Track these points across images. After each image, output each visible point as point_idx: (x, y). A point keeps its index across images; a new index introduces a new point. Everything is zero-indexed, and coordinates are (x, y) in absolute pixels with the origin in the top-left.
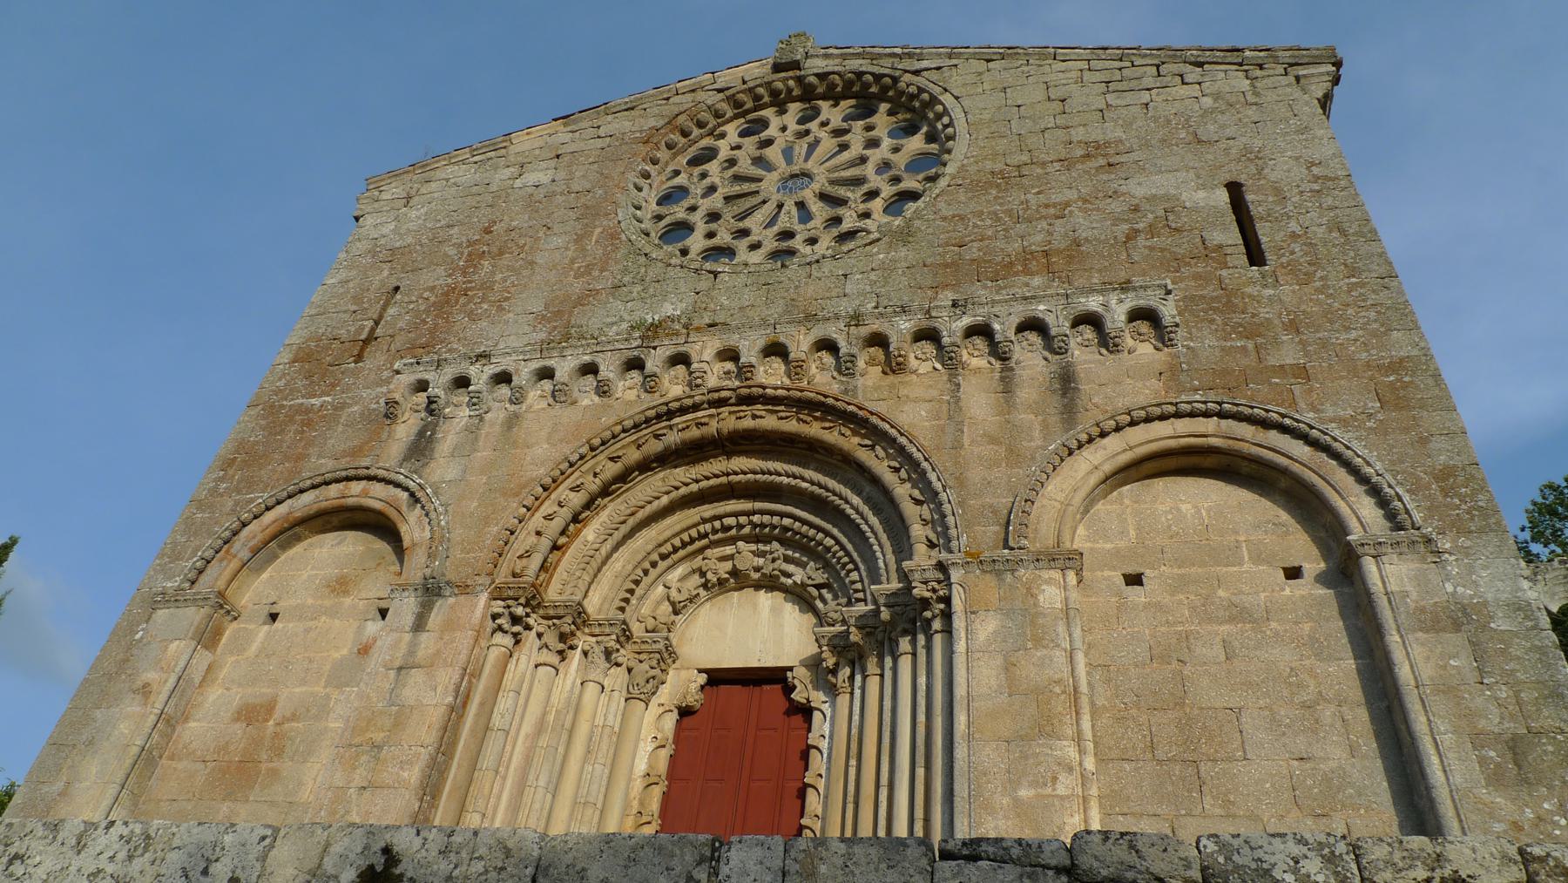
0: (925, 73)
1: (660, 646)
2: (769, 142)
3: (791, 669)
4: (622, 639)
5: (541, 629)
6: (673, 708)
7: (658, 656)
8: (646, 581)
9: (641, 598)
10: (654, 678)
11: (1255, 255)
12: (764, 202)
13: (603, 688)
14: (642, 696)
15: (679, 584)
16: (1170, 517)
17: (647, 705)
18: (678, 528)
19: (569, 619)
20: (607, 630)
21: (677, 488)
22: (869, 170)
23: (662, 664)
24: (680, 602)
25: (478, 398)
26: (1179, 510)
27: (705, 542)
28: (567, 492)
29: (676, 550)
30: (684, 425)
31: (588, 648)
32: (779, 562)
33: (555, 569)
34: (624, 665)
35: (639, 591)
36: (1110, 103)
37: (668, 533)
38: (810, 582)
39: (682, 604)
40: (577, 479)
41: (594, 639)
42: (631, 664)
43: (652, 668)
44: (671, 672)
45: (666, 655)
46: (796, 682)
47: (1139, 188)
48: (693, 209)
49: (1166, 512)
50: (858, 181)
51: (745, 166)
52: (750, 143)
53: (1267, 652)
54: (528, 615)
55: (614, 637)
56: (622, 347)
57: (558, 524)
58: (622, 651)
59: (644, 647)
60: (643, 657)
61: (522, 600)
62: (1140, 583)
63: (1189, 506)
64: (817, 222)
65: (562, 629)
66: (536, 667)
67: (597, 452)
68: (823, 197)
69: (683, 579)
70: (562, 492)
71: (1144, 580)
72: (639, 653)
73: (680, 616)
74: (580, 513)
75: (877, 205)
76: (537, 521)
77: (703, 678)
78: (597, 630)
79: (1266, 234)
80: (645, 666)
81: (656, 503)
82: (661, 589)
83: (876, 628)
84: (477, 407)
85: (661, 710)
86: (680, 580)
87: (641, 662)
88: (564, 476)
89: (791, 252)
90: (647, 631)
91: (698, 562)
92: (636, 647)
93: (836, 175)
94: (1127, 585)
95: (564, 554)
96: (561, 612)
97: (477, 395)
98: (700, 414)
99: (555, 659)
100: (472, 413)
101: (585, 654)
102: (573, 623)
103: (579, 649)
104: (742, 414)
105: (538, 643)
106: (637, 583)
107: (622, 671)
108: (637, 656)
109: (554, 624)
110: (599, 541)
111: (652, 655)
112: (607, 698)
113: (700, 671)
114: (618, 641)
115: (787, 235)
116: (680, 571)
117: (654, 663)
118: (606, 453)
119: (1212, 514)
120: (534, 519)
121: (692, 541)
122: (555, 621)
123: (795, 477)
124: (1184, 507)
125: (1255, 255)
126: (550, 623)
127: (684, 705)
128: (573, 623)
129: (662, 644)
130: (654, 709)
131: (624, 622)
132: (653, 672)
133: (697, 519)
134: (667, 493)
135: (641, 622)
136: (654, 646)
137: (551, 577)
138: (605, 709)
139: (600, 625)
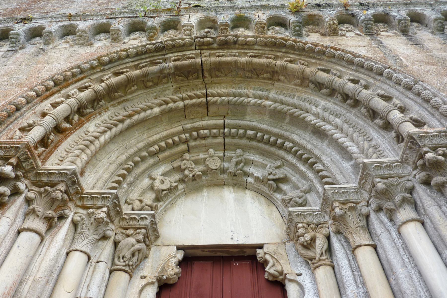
1: (147, 222)
3: (261, 247)
4: (112, 213)
5: (31, 195)
6: (155, 280)
7: (143, 231)
8: (138, 171)
9: (131, 184)
10: (139, 250)
13: (89, 258)
14: (127, 269)
15: (162, 177)
17: (131, 277)
18: (165, 133)
19: (62, 187)
20: (99, 203)
21: (167, 103)
23: (147, 240)
24: (163, 190)
25: (16, 38)
27: (183, 147)
28: (76, 90)
29: (161, 150)
30: (176, 58)
31: (79, 219)
32: (242, 164)
33: (56, 147)
34: (112, 239)
35: (130, 179)
37: (157, 137)
38: (271, 177)
39: (165, 192)
40: (86, 82)
41: (84, 212)
42: (119, 237)
43: (138, 242)
44: (153, 249)
45: (150, 232)
46: (268, 257)
54: (17, 178)
55: (105, 209)
56: (130, 16)
57: (62, 109)
58: (111, 226)
59: (131, 223)
60: (130, 232)
61: (13, 160)
65: (53, 195)
66: (19, 232)
67: (106, 67)
70: (72, 90)
72: (126, 229)
73: (161, 203)
74: (85, 107)
76: (46, 105)
77: (180, 255)
78: (89, 203)
80: (132, 240)
81: (149, 112)
83: (357, 203)
84: (15, 45)
85: (144, 282)
86: (163, 175)
87: (128, 236)
88: (75, 79)
90: (133, 210)
91: (176, 164)
92: (124, 224)
95: (66, 137)
96: (54, 179)
97: (15, 36)
98: (188, 53)
99: (41, 226)
100: (10, 49)
101: (75, 224)
102: (66, 192)
103: (70, 219)
105: (25, 206)
106: (129, 170)
107: (108, 246)
108: (124, 231)
109: (46, 191)
110: (99, 130)
111: (139, 231)
112: (92, 269)
113: (179, 248)
114: (108, 215)
116: (163, 169)
117: (141, 237)
118: (112, 70)
120: (43, 104)
121: (175, 144)
122: (47, 188)
123: (260, 98)
126: (42, 189)
127: (165, 277)
128: (66, 192)
129: (149, 221)
130: (138, 283)
131: (116, 197)
132: (138, 246)
133: (180, 128)
134: (160, 105)
135: (129, 204)
136: (141, 223)
137: (51, 153)
138: (88, 279)
139: (93, 198)
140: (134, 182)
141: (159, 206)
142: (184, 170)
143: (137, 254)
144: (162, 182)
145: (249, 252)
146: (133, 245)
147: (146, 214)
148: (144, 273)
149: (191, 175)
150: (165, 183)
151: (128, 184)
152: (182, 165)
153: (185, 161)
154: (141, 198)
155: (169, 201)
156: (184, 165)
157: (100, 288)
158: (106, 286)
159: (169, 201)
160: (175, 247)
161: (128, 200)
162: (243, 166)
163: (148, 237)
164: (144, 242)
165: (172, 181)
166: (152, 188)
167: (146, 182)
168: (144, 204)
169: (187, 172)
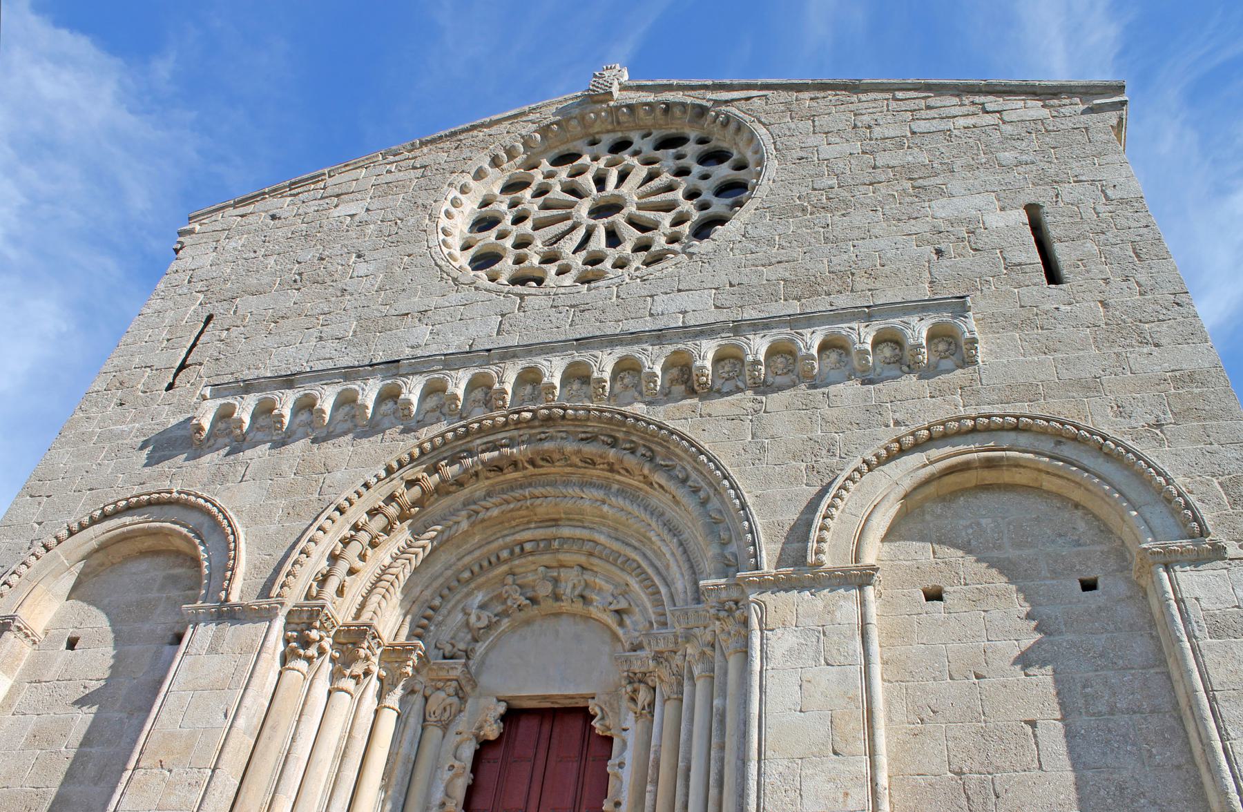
0: (735, 103)
2: (580, 172)
9: (439, 624)
11: (1053, 276)
12: (573, 228)
16: (970, 531)
22: (679, 194)
23: (460, 692)
24: (480, 629)
26: (978, 524)
36: (915, 130)
39: (482, 631)
42: (428, 692)
43: (449, 695)
47: (941, 209)
48: (501, 236)
49: (966, 527)
50: (668, 207)
51: (557, 193)
52: (563, 172)
53: (1062, 664)
62: (940, 598)
63: (990, 520)
64: (626, 248)
68: (632, 222)
69: (483, 607)
71: (944, 595)
73: (480, 644)
75: (686, 229)
77: (502, 708)
79: (1061, 252)
80: (442, 695)
82: (460, 616)
89: (600, 276)
90: (445, 657)
93: (643, 200)
94: (927, 600)
104: (543, 436)
111: (449, 683)
115: (595, 260)
117: (451, 691)
119: (1011, 527)
124: (984, 521)
125: (1053, 276)
132: (449, 700)
135: (439, 649)
138: (400, 735)
140: (443, 621)
141: (476, 648)
142: (506, 599)
143: (448, 708)
144: (479, 618)
145: (581, 704)
146: (444, 700)
147: (455, 664)
148: (460, 729)
149: (515, 606)
150: (482, 619)
151: (436, 625)
152: (504, 592)
153: (507, 587)
154: (453, 641)
155: (490, 640)
156: (506, 592)
157: (411, 744)
158: (419, 743)
159: (490, 640)
160: (495, 699)
161: (438, 645)
162: (584, 589)
163: (461, 689)
164: (457, 694)
165: (490, 615)
166: (467, 624)
167: (459, 617)
168: (455, 650)
169: (509, 603)
